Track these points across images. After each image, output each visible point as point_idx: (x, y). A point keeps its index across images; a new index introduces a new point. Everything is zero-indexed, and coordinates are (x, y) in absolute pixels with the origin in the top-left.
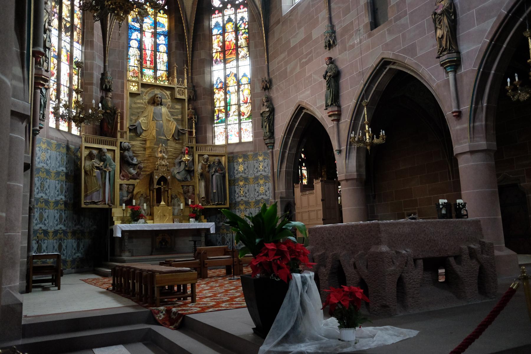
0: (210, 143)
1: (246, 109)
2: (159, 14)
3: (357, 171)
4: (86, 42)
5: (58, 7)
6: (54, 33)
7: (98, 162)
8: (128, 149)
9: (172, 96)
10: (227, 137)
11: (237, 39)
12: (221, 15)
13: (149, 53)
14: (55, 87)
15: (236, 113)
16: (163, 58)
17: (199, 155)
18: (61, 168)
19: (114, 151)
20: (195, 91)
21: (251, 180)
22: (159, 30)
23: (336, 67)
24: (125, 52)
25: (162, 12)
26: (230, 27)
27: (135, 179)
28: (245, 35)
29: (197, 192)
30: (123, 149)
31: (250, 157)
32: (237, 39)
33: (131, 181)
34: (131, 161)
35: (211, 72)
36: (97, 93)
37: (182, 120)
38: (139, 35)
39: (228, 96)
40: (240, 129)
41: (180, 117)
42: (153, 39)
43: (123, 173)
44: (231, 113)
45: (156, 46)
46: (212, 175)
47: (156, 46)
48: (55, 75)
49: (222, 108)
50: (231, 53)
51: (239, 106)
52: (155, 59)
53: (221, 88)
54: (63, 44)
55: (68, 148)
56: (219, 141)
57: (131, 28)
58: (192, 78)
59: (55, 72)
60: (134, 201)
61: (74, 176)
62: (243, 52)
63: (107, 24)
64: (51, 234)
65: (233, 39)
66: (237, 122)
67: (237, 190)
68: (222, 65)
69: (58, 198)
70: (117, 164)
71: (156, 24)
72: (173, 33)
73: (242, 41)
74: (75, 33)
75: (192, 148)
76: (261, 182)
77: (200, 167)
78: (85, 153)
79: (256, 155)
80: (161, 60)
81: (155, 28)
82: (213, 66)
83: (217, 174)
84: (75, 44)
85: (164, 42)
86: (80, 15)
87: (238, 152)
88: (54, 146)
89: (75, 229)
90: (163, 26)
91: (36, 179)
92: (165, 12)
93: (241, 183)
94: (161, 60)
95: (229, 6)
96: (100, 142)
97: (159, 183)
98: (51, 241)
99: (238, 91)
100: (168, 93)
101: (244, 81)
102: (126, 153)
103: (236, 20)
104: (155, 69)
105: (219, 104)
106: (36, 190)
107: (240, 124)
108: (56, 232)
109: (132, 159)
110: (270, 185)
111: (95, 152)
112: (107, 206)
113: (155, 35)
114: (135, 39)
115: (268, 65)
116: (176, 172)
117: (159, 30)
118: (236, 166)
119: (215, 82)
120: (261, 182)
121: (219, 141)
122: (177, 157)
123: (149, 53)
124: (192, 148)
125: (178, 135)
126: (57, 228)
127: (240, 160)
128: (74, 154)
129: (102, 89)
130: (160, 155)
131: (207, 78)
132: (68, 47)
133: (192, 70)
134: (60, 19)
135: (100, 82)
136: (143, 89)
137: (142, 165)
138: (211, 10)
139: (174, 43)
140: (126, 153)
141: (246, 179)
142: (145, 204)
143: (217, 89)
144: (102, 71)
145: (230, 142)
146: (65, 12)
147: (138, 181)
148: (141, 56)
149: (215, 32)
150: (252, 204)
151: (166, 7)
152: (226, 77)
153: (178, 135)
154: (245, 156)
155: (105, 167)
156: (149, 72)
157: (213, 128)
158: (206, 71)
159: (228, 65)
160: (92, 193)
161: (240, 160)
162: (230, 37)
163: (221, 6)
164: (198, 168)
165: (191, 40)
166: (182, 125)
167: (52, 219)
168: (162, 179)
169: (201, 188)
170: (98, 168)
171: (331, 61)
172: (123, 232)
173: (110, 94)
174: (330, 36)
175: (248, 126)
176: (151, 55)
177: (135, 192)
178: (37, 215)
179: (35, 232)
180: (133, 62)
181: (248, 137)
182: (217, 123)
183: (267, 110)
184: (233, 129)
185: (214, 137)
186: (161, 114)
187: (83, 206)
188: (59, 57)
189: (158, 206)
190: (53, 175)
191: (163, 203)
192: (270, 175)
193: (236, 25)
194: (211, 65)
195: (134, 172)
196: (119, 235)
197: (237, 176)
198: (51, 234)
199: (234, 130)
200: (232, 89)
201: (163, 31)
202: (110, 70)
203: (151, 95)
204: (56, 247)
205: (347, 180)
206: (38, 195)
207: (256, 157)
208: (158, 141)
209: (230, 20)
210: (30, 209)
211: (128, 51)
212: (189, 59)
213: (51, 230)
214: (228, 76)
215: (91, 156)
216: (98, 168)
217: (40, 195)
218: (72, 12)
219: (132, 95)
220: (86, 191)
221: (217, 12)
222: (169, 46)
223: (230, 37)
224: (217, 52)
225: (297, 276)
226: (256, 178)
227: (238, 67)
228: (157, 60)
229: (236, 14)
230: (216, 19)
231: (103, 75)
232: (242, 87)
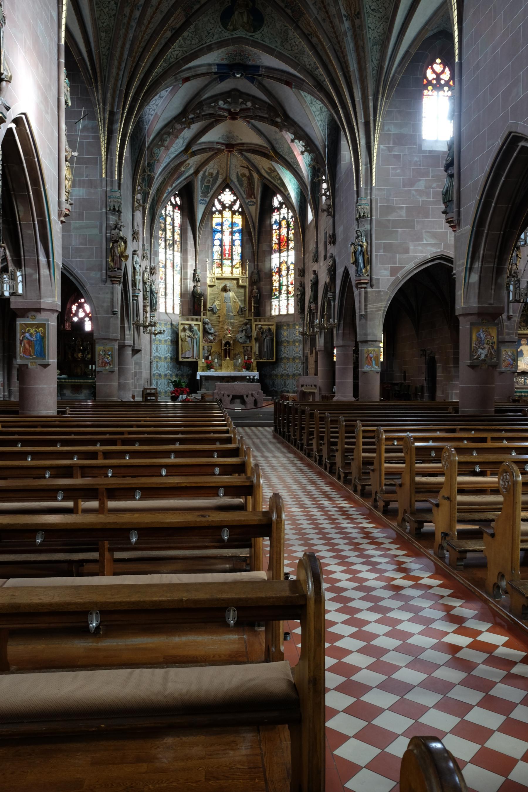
0: (268, 315)
1: (291, 289)
2: (234, 216)
3: (324, 346)
4: (184, 251)
5: (164, 233)
6: (161, 251)
7: (189, 332)
8: (207, 324)
9: (238, 283)
10: (280, 311)
11: (288, 234)
12: (278, 213)
13: (227, 248)
14: (164, 286)
15: (286, 292)
16: (237, 250)
17: (256, 325)
18: (168, 337)
19: (199, 325)
20: (259, 275)
21: (291, 343)
22: (235, 229)
23: (317, 277)
24: (210, 251)
25: (237, 214)
26: (284, 223)
27: (212, 343)
28: (293, 231)
29: (253, 351)
30: (204, 324)
31: (291, 326)
32: (288, 234)
33: (210, 344)
34: (209, 331)
35: (270, 260)
36: (190, 285)
37: (245, 301)
38: (220, 235)
39: (281, 279)
40: (288, 304)
41: (243, 298)
42: (231, 237)
43: (205, 339)
44: (283, 292)
45: (233, 241)
46: (264, 339)
47: (233, 241)
48: (164, 279)
49: (277, 287)
50: (284, 245)
51: (288, 286)
52: (232, 251)
53: (277, 272)
54: (167, 257)
55: (172, 324)
56: (275, 312)
57: (215, 231)
58: (257, 265)
59: (164, 277)
60: (210, 357)
61: (175, 341)
62: (292, 244)
63: (196, 235)
64: (163, 376)
65: (286, 233)
66: (286, 298)
67: (283, 349)
68: (278, 254)
69: (166, 356)
70: (200, 334)
71: (233, 224)
72: (245, 230)
73: (291, 236)
74: (176, 246)
75: (251, 320)
76: (297, 344)
77: (256, 334)
78: (181, 328)
79: (294, 325)
80: (236, 252)
81: (232, 228)
82: (272, 254)
83: (268, 338)
84: (175, 253)
85: (239, 238)
86: (179, 232)
87: (284, 322)
88: (163, 325)
89: (178, 373)
90: (238, 225)
91: (153, 346)
92: (240, 213)
93: (285, 344)
94: (236, 252)
95: (284, 206)
96: (188, 320)
97: (225, 345)
98: (163, 380)
99: (287, 275)
100: (235, 282)
101: (292, 267)
102: (206, 326)
103: (288, 218)
104: (232, 260)
105: (276, 285)
106: (153, 352)
107: (288, 300)
108: (166, 375)
109: (210, 330)
110: (301, 346)
111: (187, 327)
112: (195, 360)
113: (232, 233)
114: (218, 239)
115: (304, 258)
116: (239, 337)
117: (235, 229)
118: (282, 332)
119: (273, 268)
120: (297, 344)
121: (275, 312)
122: (240, 327)
123: (227, 248)
124: (251, 320)
125: (241, 311)
126: (167, 372)
127: (285, 328)
128: (176, 328)
129: (193, 280)
130: (226, 327)
131: (267, 266)
132: (171, 258)
133: (257, 258)
134: (166, 241)
135: (192, 276)
136: (218, 281)
137: (217, 334)
138: (272, 209)
139: (245, 238)
140: (206, 326)
141: (288, 342)
142: (216, 360)
143: (275, 272)
144: (194, 268)
145: (281, 313)
146: (169, 234)
147: (214, 343)
148: (222, 251)
149: (275, 227)
150: (291, 360)
151: (240, 210)
152: (281, 263)
153: (242, 311)
154: (288, 325)
155: (194, 335)
156: (227, 263)
157: (271, 303)
158: (266, 260)
159: (282, 254)
160: (185, 352)
161: (285, 328)
162: (284, 232)
163: (279, 206)
164: (254, 334)
165: (256, 237)
166: (245, 304)
167: (164, 367)
168: (228, 343)
169: (256, 348)
170: (189, 336)
171: (314, 271)
172: (201, 377)
173: (199, 284)
174: (315, 256)
175: (292, 301)
176: (229, 249)
177: (212, 351)
178: (154, 365)
179: (154, 375)
180: (217, 256)
181: (292, 311)
182: (274, 299)
183: (299, 293)
184: (284, 303)
185: (271, 309)
186: (230, 298)
187: (180, 360)
188: (165, 267)
189: (225, 360)
190: (163, 342)
191: (228, 358)
192: (302, 339)
193: (287, 222)
194: (271, 254)
195: (211, 338)
196: (198, 378)
197: (283, 339)
198: (163, 376)
199: (283, 305)
200: (284, 273)
201: (238, 230)
202: (200, 266)
203: (223, 285)
204: (166, 383)
205: (319, 351)
206: (154, 354)
207: (295, 326)
208: (227, 316)
209: (284, 218)
210: (151, 363)
211: (212, 248)
212: (255, 250)
213: (163, 374)
214: (282, 263)
215: (184, 330)
216: (189, 336)
217: (156, 354)
218: (173, 232)
219: (211, 286)
220: (182, 351)
221: (276, 211)
222: (242, 241)
223: (284, 232)
224: (275, 244)
225: (181, 396)
226: (294, 341)
227: (288, 256)
228: (234, 253)
229: (288, 213)
230: (275, 217)
231: (195, 270)
232: (290, 272)
